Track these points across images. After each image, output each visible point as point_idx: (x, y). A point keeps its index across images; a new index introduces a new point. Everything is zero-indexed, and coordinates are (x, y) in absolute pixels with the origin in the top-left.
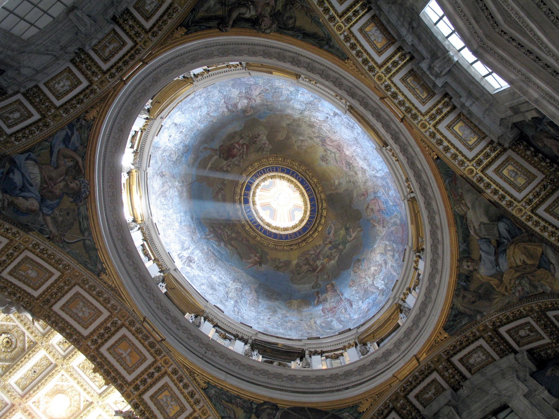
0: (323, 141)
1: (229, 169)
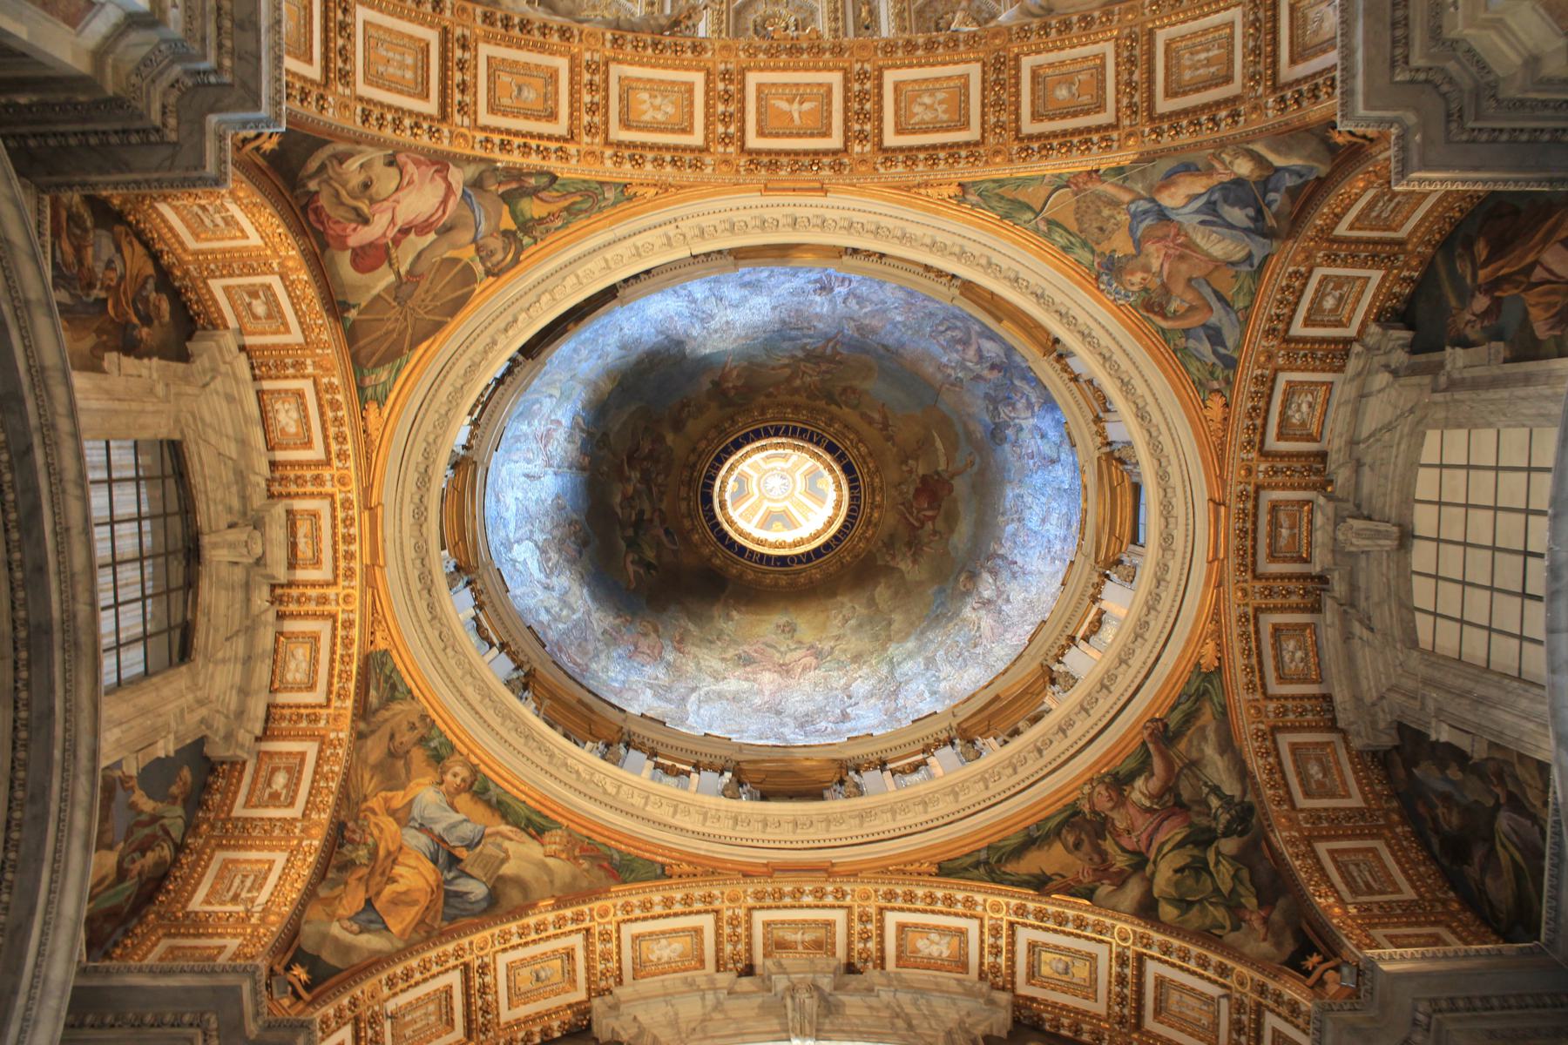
0: (818, 654)
1: (905, 468)
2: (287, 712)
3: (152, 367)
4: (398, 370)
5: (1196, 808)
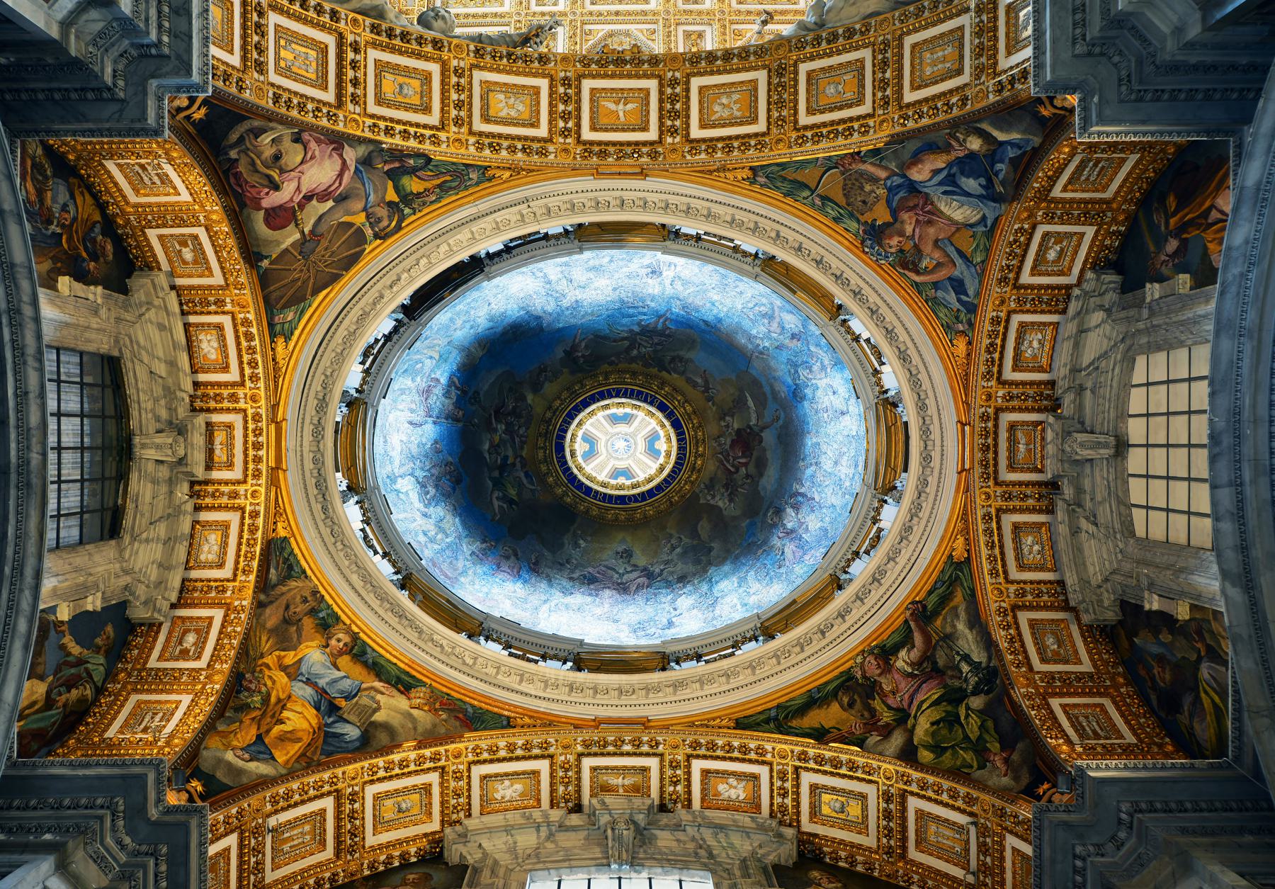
2: (199, 584)
3: (97, 293)
4: (302, 313)
5: (950, 673)
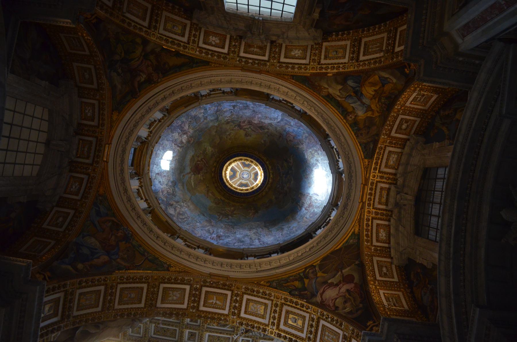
3: (419, 260)
4: (347, 242)
